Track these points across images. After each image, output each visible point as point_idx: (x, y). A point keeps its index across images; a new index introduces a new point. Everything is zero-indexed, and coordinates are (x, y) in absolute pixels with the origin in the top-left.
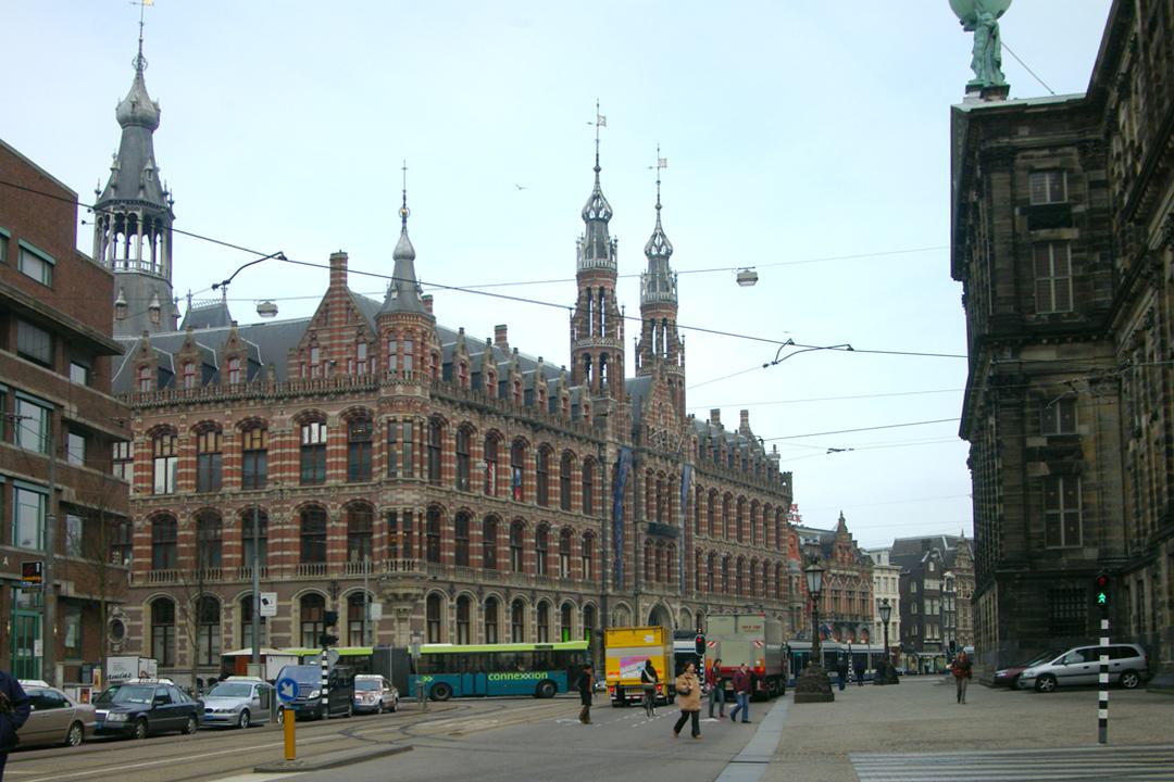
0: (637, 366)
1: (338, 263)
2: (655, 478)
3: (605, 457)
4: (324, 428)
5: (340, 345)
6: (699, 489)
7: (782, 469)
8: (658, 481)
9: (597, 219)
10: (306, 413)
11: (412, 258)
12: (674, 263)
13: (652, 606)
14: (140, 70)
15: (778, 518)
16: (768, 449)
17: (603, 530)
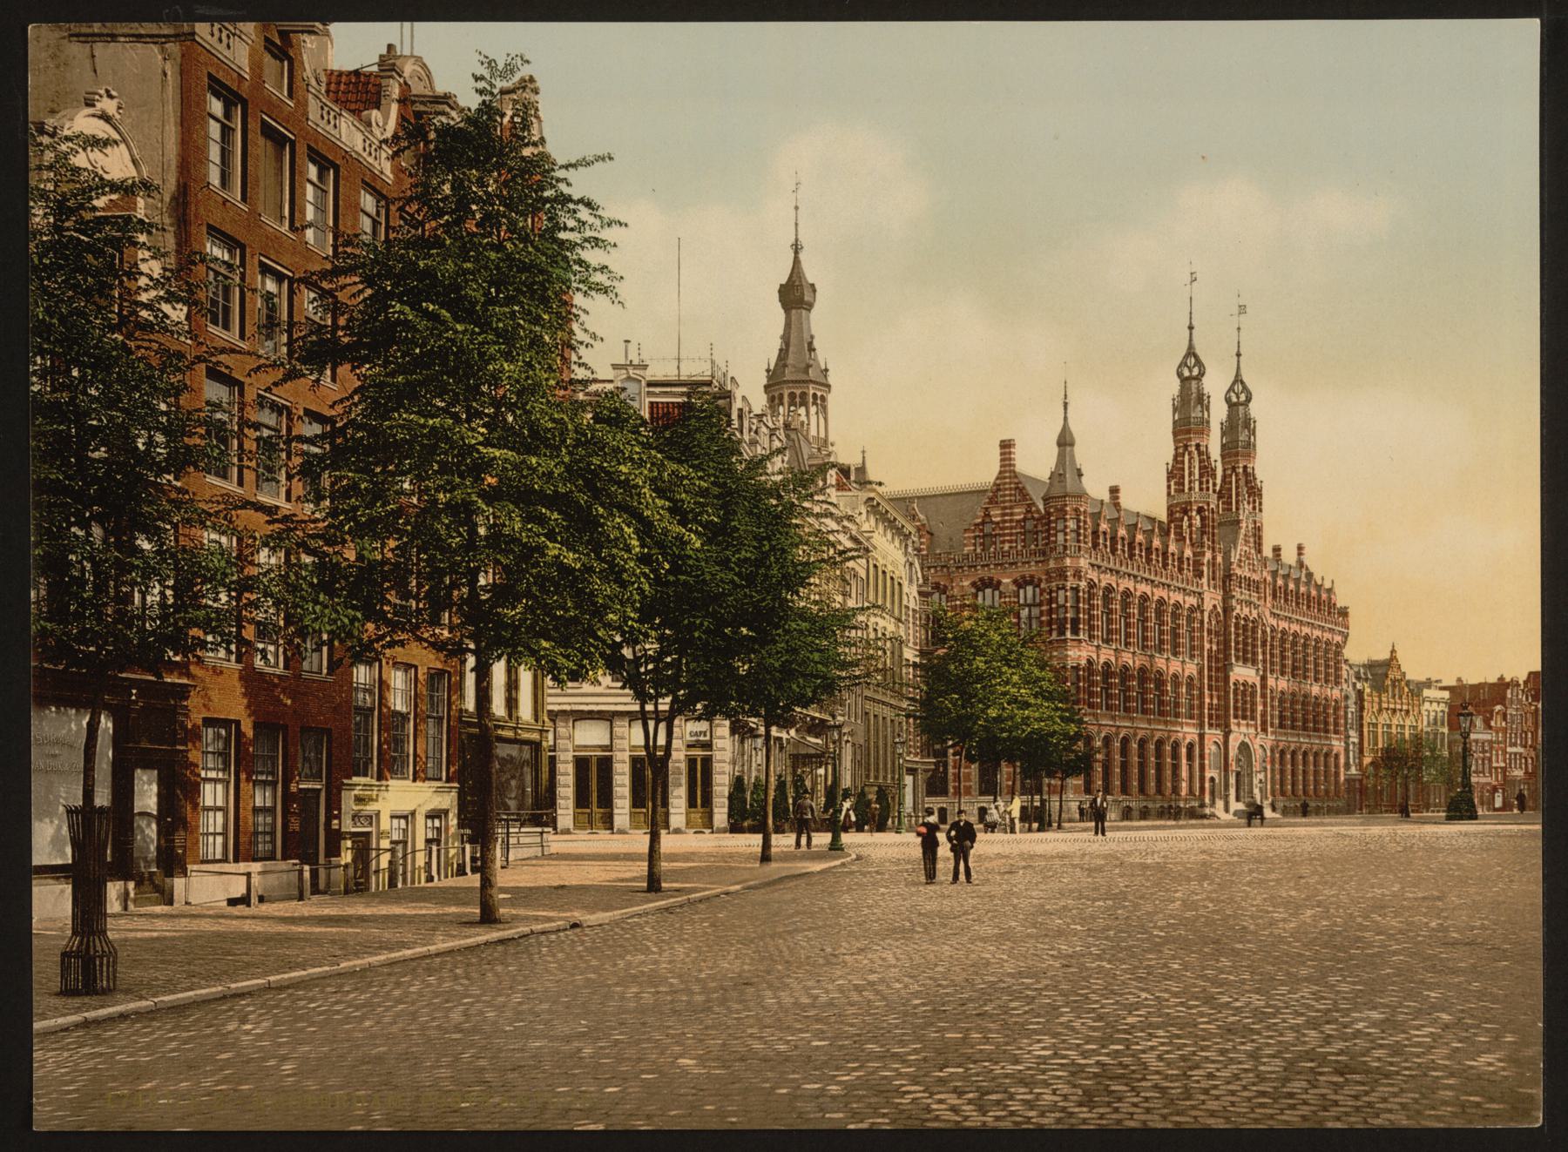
0: (1169, 494)
1: (1006, 446)
4: (997, 593)
5: (1011, 521)
6: (1273, 630)
7: (1338, 606)
9: (1191, 371)
10: (981, 580)
11: (1072, 444)
12: (1255, 409)
14: (796, 253)
15: (1338, 653)
16: (1327, 585)
17: (1201, 672)
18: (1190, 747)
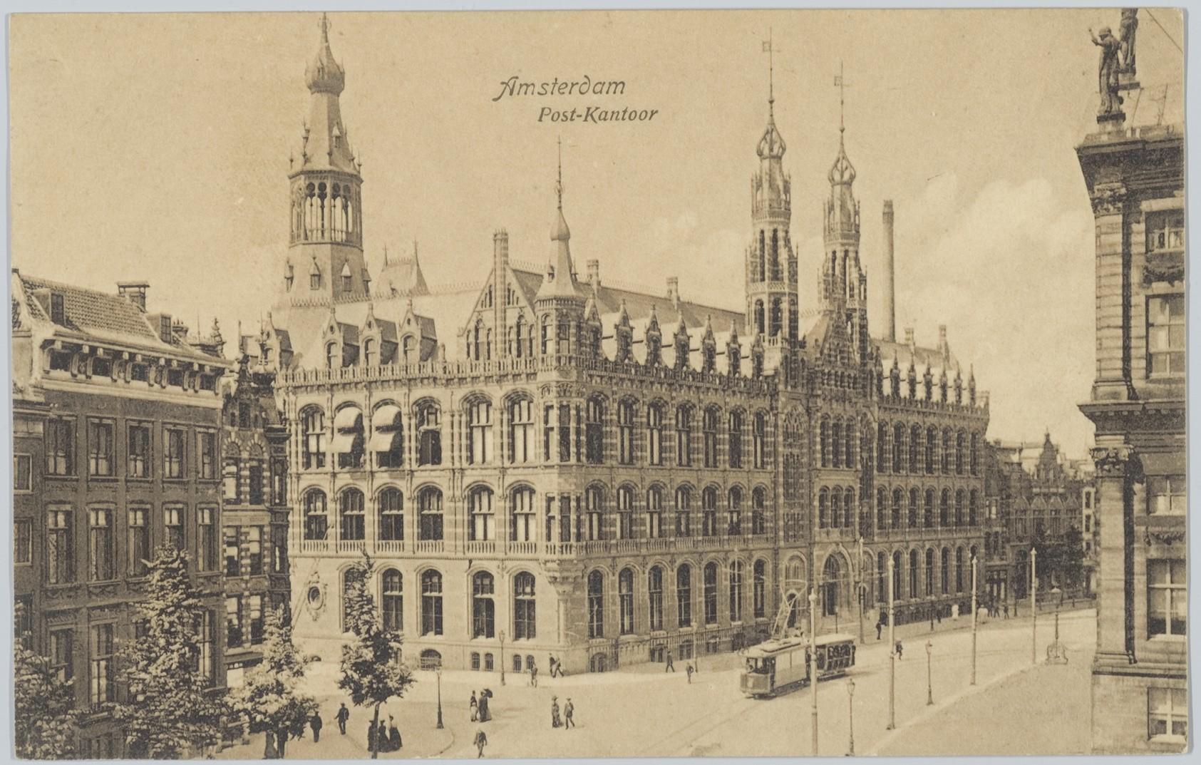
2: (831, 422)
3: (777, 408)
8: (835, 425)
13: (827, 555)
17: (775, 483)
18: (759, 566)
